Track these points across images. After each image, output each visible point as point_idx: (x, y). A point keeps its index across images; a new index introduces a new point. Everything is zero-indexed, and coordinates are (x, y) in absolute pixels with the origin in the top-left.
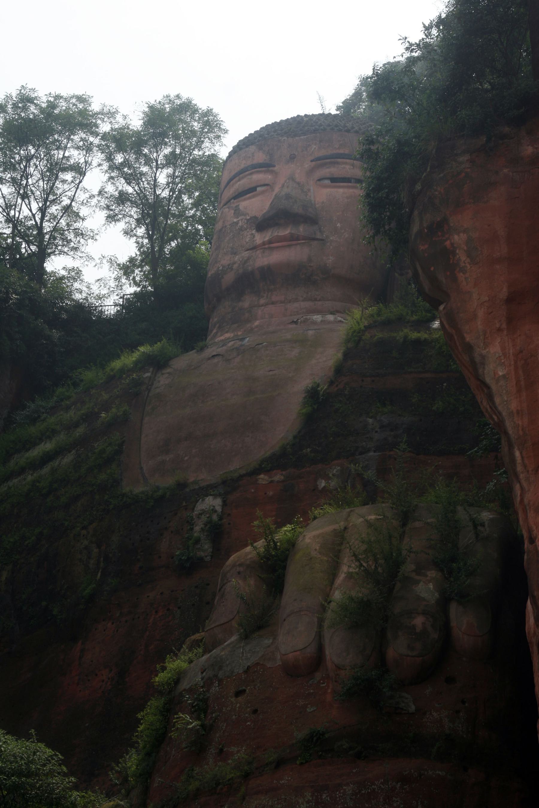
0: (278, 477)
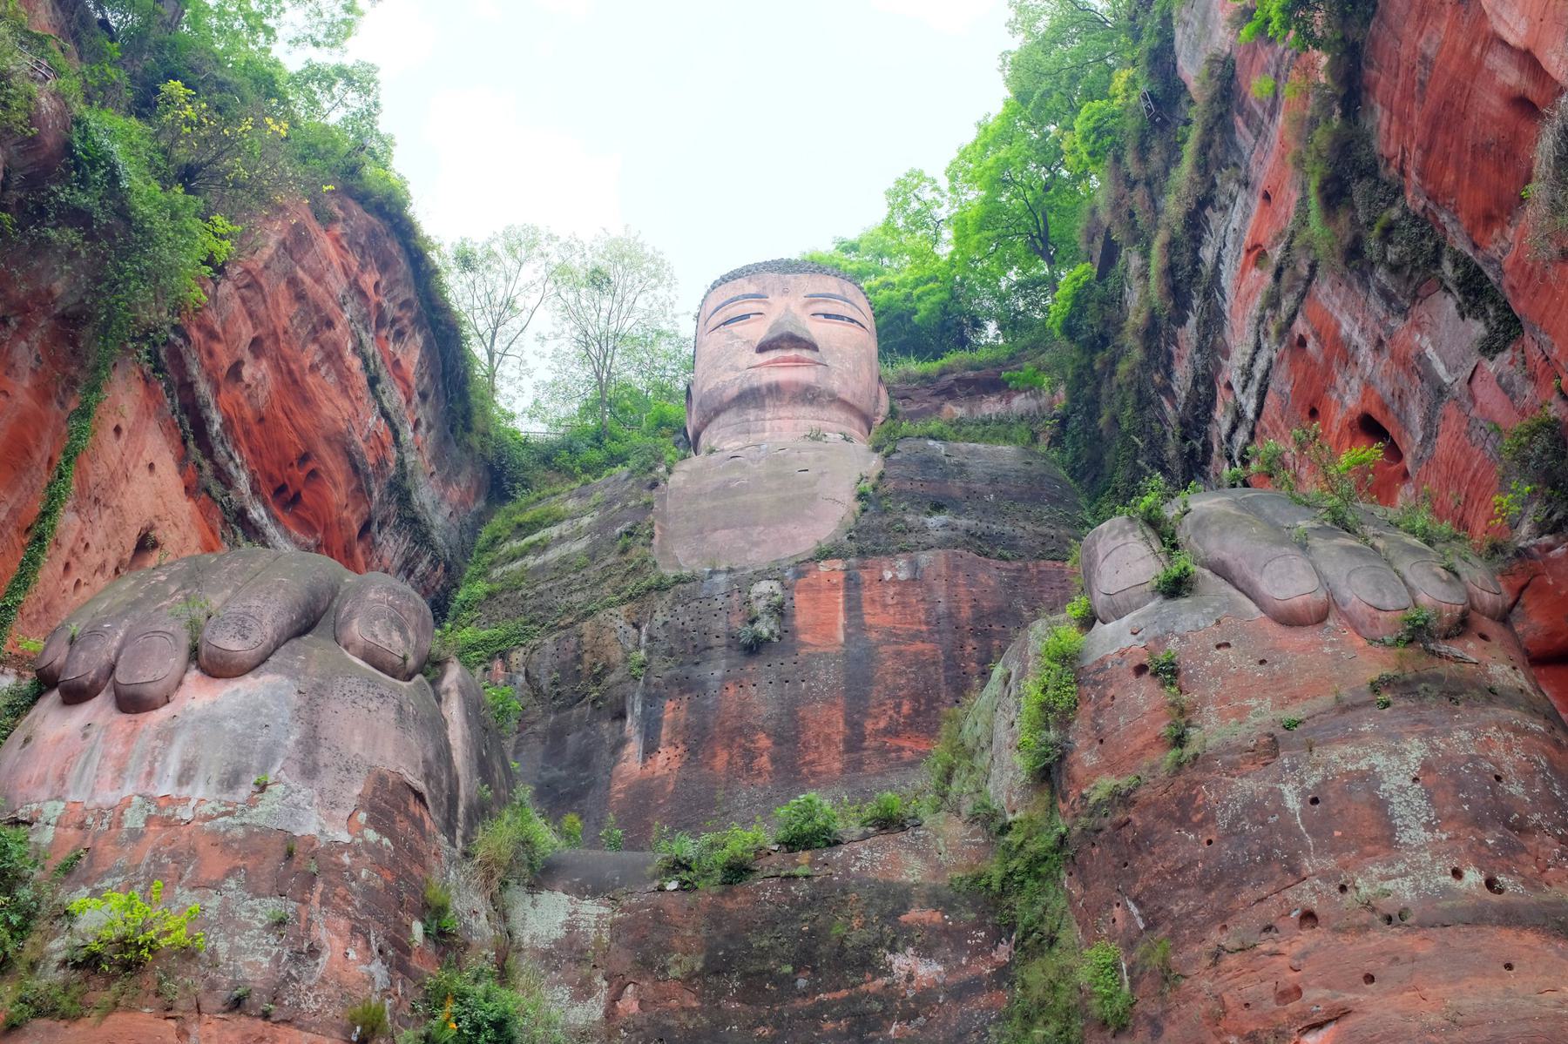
0: (839, 565)
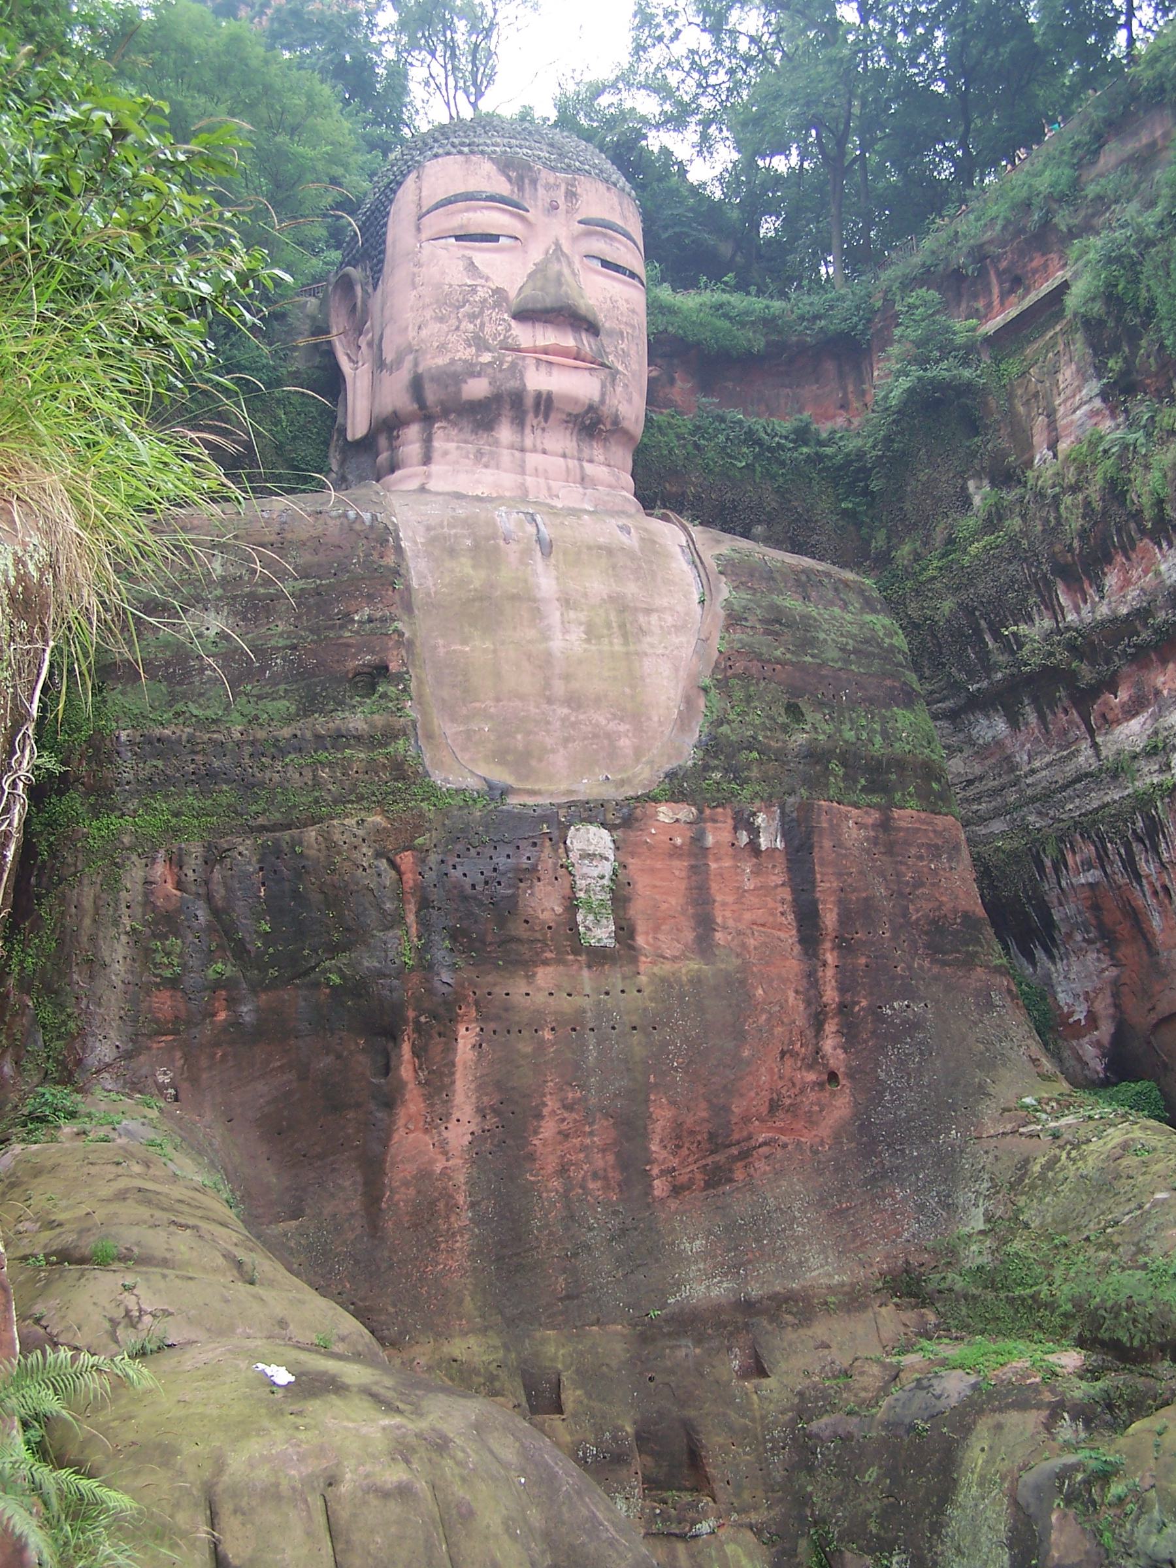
0: (686, 812)
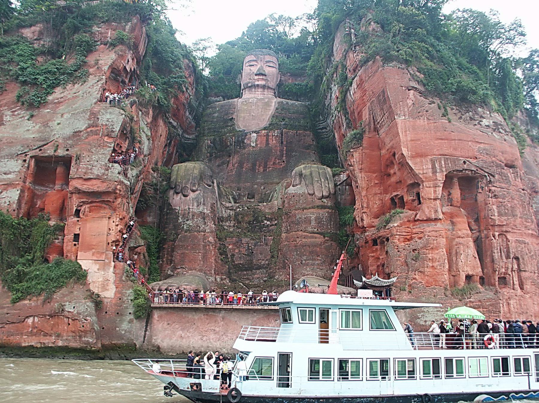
0: (266, 131)
